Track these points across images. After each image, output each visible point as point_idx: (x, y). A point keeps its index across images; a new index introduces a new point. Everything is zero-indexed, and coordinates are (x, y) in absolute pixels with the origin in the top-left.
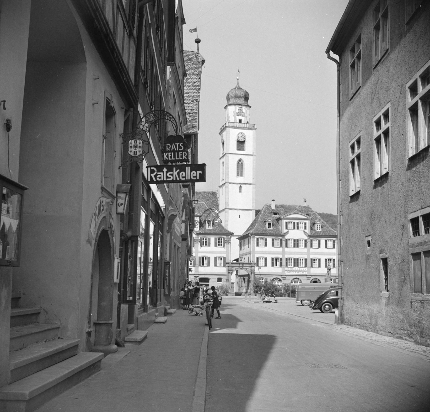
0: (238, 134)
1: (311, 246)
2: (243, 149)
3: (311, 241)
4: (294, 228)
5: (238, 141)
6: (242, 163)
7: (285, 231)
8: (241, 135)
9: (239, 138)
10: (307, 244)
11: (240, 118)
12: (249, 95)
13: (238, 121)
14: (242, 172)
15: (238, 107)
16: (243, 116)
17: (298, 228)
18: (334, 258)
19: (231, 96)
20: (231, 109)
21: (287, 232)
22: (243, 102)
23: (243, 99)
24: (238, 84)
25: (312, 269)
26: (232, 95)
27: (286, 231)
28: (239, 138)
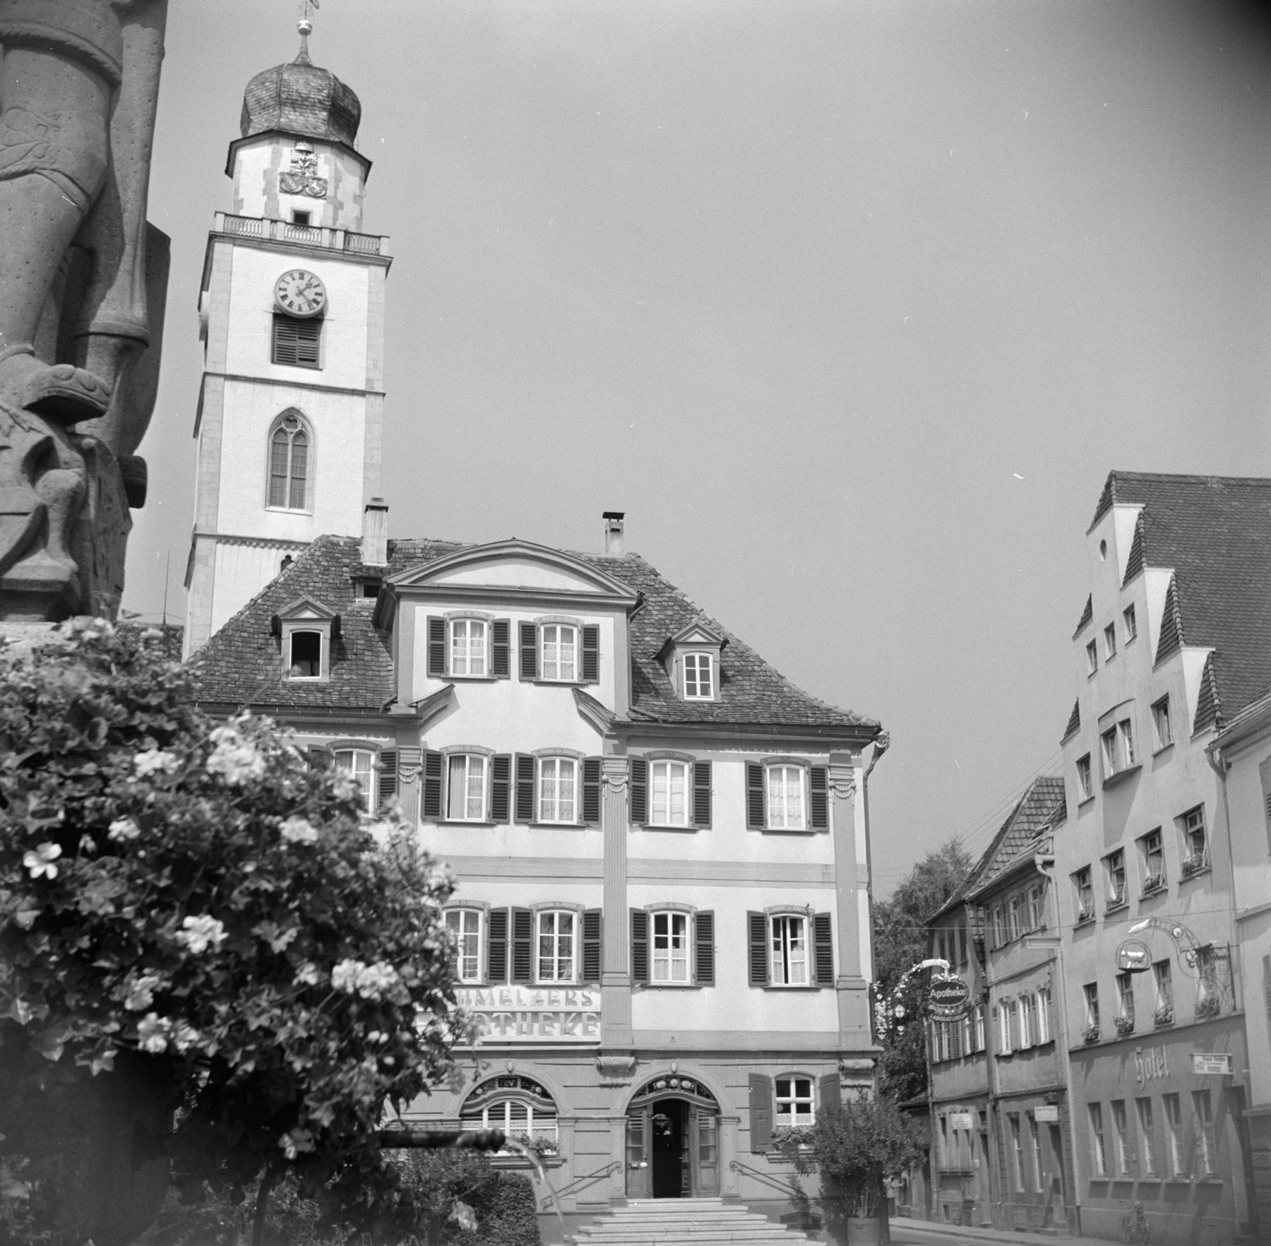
0: (282, 279)
1: (639, 811)
2: (310, 360)
3: (639, 770)
4: (500, 666)
5: (281, 317)
6: (301, 434)
7: (424, 686)
8: (302, 284)
9: (284, 297)
10: (605, 791)
11: (303, 203)
12: (357, 102)
13: (290, 219)
14: (299, 479)
15: (288, 153)
16: (316, 196)
17: (529, 669)
18: (819, 909)
19: (258, 101)
20: (254, 159)
21: (440, 704)
22: (322, 129)
23: (324, 114)
24: (304, 52)
25: (641, 1001)
26: (263, 94)
27: (437, 685)
28: (284, 297)
